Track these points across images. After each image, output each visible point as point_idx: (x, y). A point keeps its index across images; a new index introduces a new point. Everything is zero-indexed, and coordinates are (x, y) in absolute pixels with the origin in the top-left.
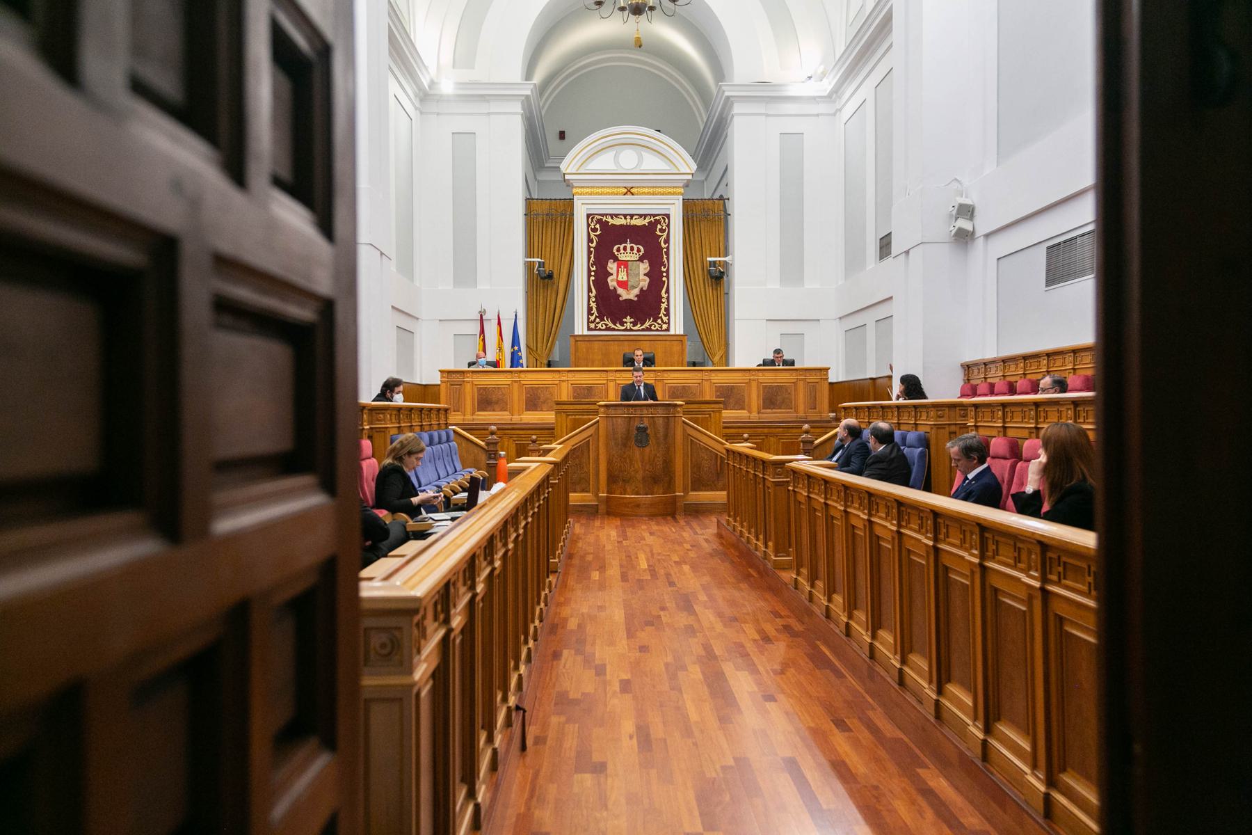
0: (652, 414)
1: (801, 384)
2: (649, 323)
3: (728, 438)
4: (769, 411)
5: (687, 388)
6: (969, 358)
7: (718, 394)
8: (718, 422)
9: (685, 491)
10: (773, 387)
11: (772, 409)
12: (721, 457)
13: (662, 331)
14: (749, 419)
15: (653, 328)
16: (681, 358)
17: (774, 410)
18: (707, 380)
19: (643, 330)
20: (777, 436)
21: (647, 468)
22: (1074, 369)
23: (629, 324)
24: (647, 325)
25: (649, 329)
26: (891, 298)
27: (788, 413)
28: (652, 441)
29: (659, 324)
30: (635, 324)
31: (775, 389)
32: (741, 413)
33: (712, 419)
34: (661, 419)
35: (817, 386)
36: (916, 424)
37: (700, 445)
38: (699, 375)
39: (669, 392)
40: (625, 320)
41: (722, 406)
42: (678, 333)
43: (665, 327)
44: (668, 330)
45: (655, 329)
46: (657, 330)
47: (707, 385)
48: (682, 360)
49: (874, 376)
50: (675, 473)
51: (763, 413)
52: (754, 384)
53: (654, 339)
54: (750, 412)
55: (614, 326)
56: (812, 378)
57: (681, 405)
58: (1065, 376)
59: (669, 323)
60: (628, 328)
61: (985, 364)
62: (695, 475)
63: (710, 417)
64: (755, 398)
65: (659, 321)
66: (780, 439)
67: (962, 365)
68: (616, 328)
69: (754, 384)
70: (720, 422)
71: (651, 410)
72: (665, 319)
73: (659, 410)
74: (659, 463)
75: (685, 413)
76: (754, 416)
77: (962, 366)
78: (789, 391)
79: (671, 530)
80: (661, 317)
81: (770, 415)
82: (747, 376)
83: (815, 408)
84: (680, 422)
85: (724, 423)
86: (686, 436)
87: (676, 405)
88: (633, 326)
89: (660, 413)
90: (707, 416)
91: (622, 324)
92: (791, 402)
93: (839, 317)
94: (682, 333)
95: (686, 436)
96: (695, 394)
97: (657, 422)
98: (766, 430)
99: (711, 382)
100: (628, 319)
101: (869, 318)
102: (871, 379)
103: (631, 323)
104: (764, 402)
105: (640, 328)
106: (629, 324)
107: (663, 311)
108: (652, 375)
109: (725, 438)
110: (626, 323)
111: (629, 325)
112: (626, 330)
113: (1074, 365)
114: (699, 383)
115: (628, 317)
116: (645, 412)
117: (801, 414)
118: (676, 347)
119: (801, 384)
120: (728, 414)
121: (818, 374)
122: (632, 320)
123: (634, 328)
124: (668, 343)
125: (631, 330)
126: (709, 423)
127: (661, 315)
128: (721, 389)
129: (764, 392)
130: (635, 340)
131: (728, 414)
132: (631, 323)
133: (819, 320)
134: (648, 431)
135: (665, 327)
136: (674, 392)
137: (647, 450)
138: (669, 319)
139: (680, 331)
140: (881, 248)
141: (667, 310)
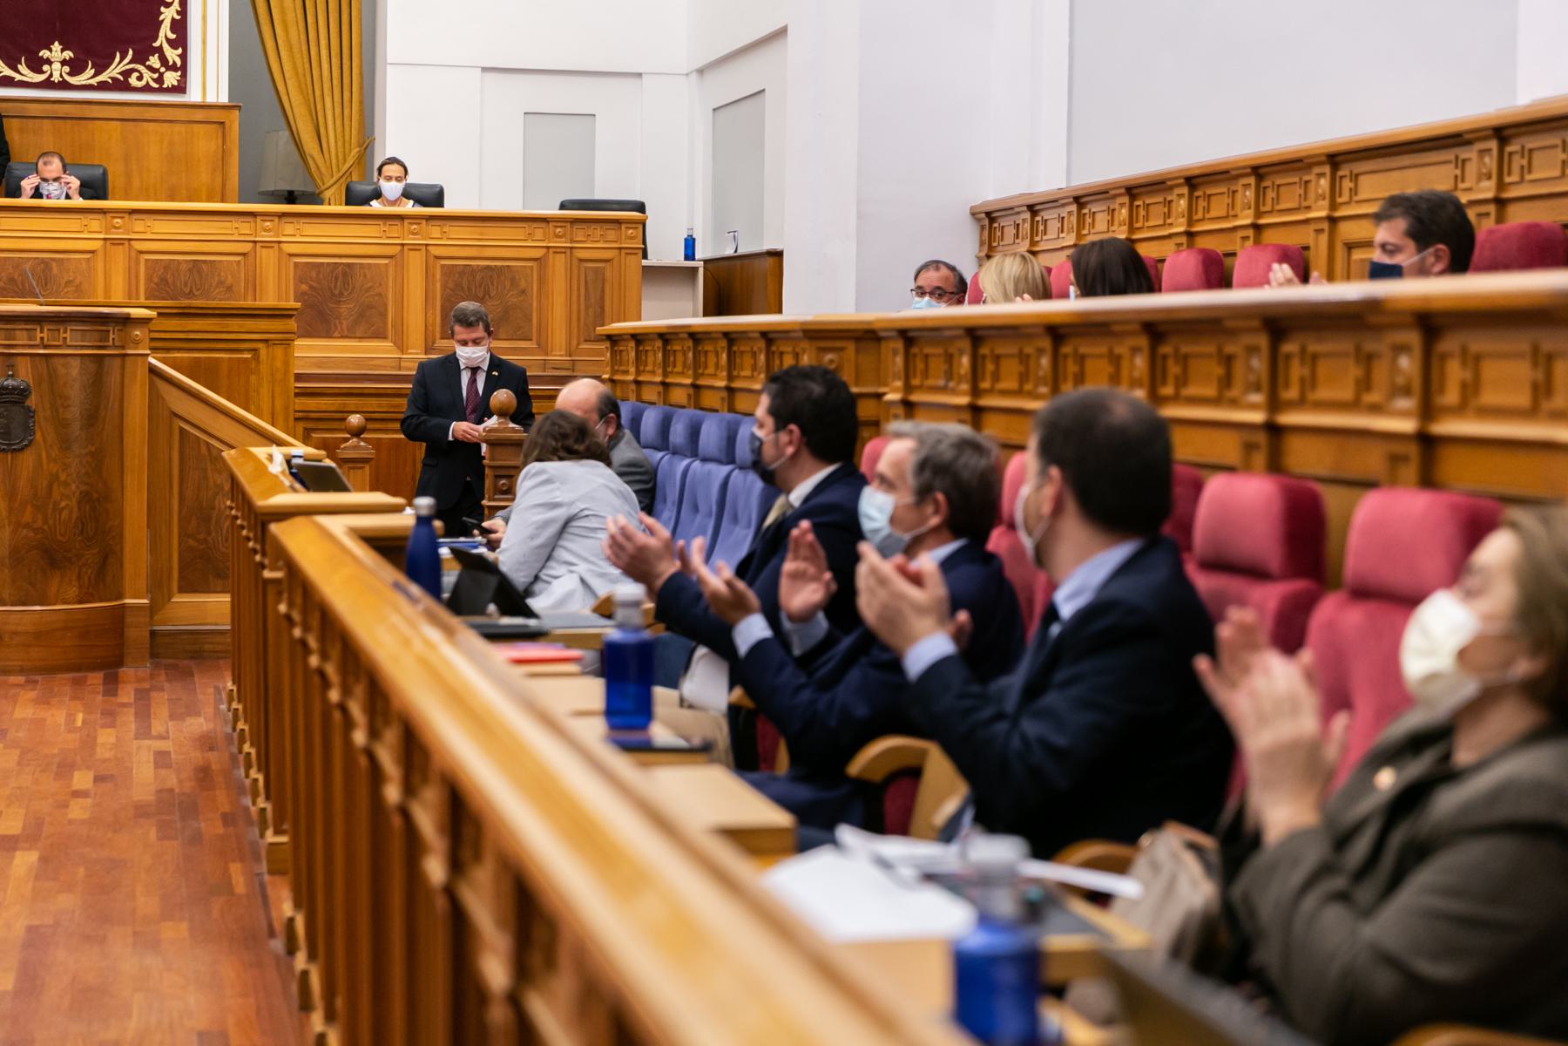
0: (46, 347)
1: (559, 264)
2: (123, 67)
3: (310, 425)
5: (205, 267)
6: (993, 192)
7: (304, 287)
8: (279, 376)
9: (158, 589)
10: (472, 271)
13: (161, 90)
15: (133, 81)
16: (219, 180)
18: (267, 245)
19: (103, 87)
21: (27, 516)
22: (1257, 228)
23: (56, 66)
24: (114, 71)
25: (120, 85)
28: (44, 432)
29: (151, 69)
30: (76, 67)
31: (478, 277)
32: (376, 350)
33: (264, 368)
34: (76, 363)
35: (608, 274)
36: (696, 387)
37: (207, 443)
38: (245, 227)
39: (149, 279)
40: (44, 53)
41: (292, 324)
42: (211, 99)
43: (171, 78)
44: (180, 88)
45: (143, 83)
46: (147, 89)
47: (267, 258)
48: (224, 185)
50: (121, 536)
52: (415, 263)
53: (134, 118)
54: (401, 346)
55: (8, 72)
56: (594, 246)
57: (144, 321)
58: (1229, 249)
59: (183, 69)
60: (56, 78)
61: (1033, 209)
62: (191, 542)
63: (256, 358)
65: (154, 61)
67: (974, 214)
68: (18, 77)
69: (415, 263)
70: (286, 373)
71: (42, 334)
72: (172, 55)
73: (69, 334)
74: (67, 503)
75: (159, 345)
77: (973, 214)
78: (523, 284)
79: (71, 718)
80: (160, 50)
82: (395, 235)
84: (142, 374)
85: (299, 378)
86: (159, 414)
87: (126, 320)
88: (71, 74)
89: (74, 342)
90: (247, 356)
91: (36, 65)
92: (531, 320)
94: (224, 99)
95: (159, 414)
96: (229, 289)
97: (61, 370)
99: (280, 249)
100: (56, 53)
103: (64, 63)
105: (94, 82)
106: (56, 66)
107: (165, 31)
108: (95, 223)
109: (301, 426)
110: (49, 62)
111: (57, 71)
112: (48, 84)
113: (1259, 214)
114: (244, 254)
115: (56, 46)
116: (21, 338)
118: (205, 143)
119: (559, 264)
120: (311, 352)
121: (611, 235)
122: (68, 54)
123: (74, 80)
124: (178, 128)
125: (63, 85)
126: (253, 378)
127: (161, 41)
128: (314, 274)
129: (444, 287)
130: (79, 117)
131: (311, 352)
132: (64, 63)
134: (32, 401)
135: (171, 78)
136: (163, 280)
137: (27, 459)
138: (184, 57)
139: (219, 93)
141: (180, 26)
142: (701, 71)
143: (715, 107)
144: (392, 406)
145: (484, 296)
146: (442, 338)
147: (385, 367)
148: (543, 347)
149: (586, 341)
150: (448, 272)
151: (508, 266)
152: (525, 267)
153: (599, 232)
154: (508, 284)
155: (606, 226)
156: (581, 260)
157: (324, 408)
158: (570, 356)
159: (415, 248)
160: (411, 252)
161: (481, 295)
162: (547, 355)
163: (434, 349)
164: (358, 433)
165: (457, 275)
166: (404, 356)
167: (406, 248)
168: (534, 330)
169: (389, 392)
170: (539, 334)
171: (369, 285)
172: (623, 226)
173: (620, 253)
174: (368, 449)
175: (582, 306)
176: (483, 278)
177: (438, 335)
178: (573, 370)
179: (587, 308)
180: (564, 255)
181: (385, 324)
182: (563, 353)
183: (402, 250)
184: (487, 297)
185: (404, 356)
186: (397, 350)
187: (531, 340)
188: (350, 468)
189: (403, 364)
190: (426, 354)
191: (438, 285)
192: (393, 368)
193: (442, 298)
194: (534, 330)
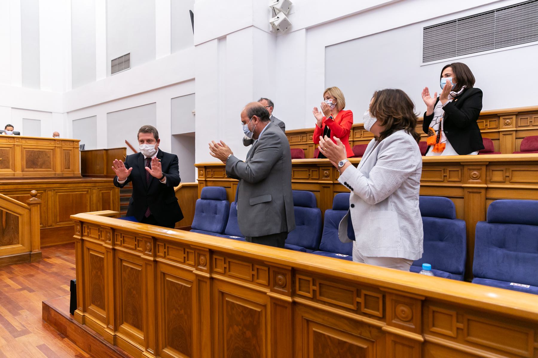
4: (32, 169)
10: (35, 152)
11: (34, 168)
12: (7, 212)
14: (14, 176)
17: (35, 169)
20: (54, 190)
26: (193, 79)
27: (47, 171)
31: (36, 154)
49: (106, 148)
51: (26, 171)
52: (18, 150)
56: (67, 146)
64: (19, 160)
66: (56, 192)
69: (18, 150)
76: (19, 173)
78: (49, 155)
81: (32, 172)
82: (11, 142)
83: (69, 168)
92: (51, 163)
93: (68, 111)
98: (44, 186)
101: (101, 113)
102: (105, 150)
104: (27, 163)
117: (59, 171)
119: (58, 151)
121: (71, 144)
129: (27, 155)
133: (51, 113)
140: (112, 67)
142: (68, 113)
143: (73, 120)
144: (32, 187)
145: (38, 158)
146: (26, 168)
147: (8, 176)
148: (54, 170)
149: (66, 169)
150: (27, 152)
151: (45, 151)
152: (49, 151)
153: (68, 143)
154: (45, 155)
155: (71, 142)
156: (64, 150)
157: (10, 188)
158: (62, 172)
159: (18, 145)
160: (17, 147)
161: (37, 157)
162: (55, 171)
163: (24, 171)
164: (35, 196)
165: (30, 153)
166: (15, 173)
167: (15, 145)
168: (52, 166)
169: (31, 183)
170: (53, 167)
171: (4, 155)
172: (75, 142)
173: (74, 149)
174: (39, 200)
175: (64, 161)
176: (37, 154)
177: (25, 168)
178: (63, 175)
179: (66, 161)
180: (59, 149)
181: (9, 165)
182: (60, 171)
183: (14, 146)
184: (39, 158)
185: (15, 173)
186: (12, 171)
187: (51, 168)
188: (33, 206)
189: (15, 175)
190: (22, 172)
191: (25, 155)
192: (12, 176)
193: (26, 158)
194: (52, 166)
